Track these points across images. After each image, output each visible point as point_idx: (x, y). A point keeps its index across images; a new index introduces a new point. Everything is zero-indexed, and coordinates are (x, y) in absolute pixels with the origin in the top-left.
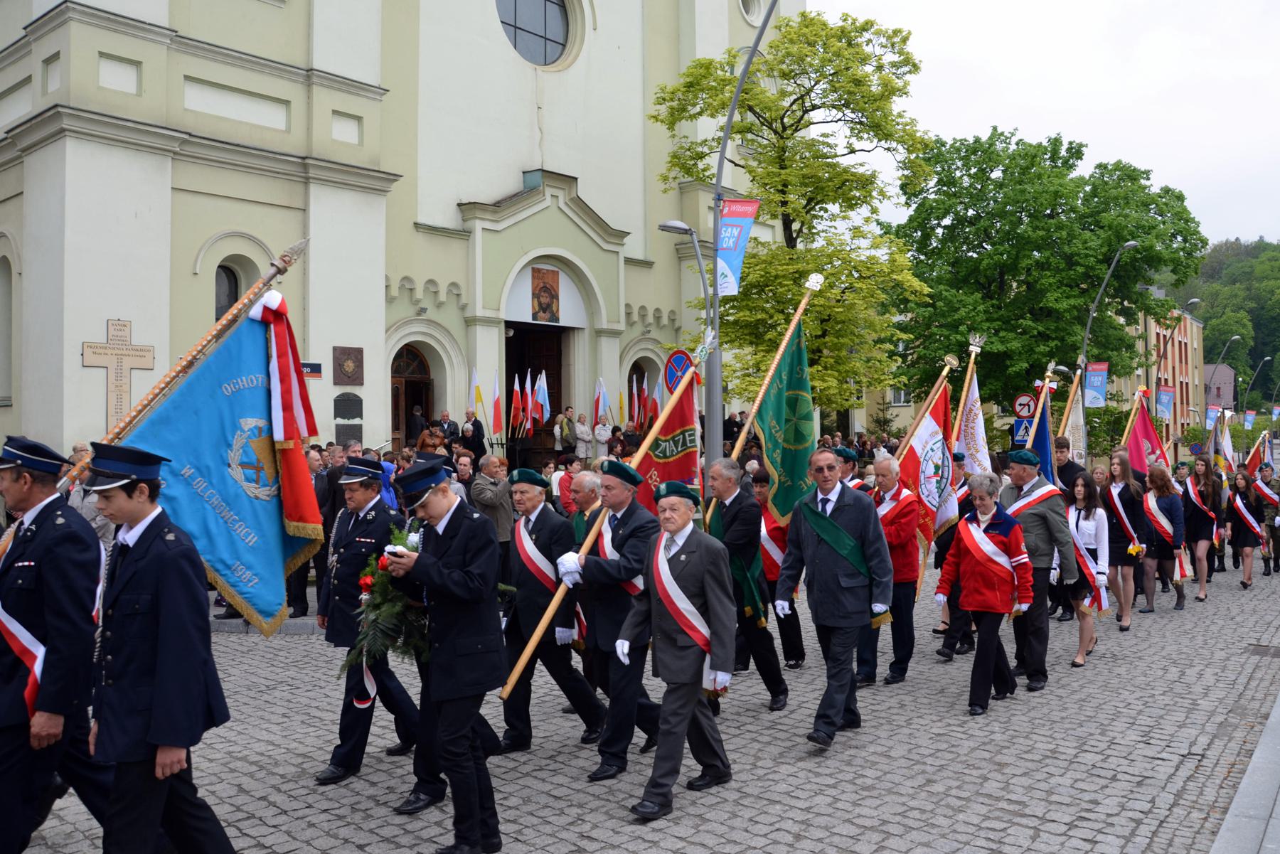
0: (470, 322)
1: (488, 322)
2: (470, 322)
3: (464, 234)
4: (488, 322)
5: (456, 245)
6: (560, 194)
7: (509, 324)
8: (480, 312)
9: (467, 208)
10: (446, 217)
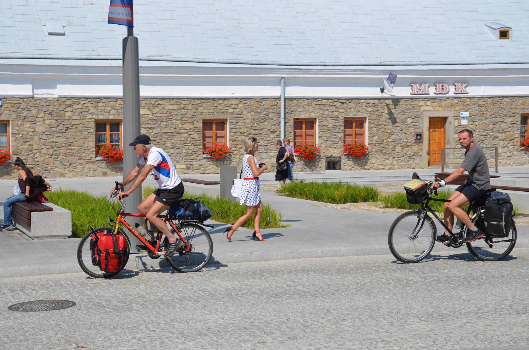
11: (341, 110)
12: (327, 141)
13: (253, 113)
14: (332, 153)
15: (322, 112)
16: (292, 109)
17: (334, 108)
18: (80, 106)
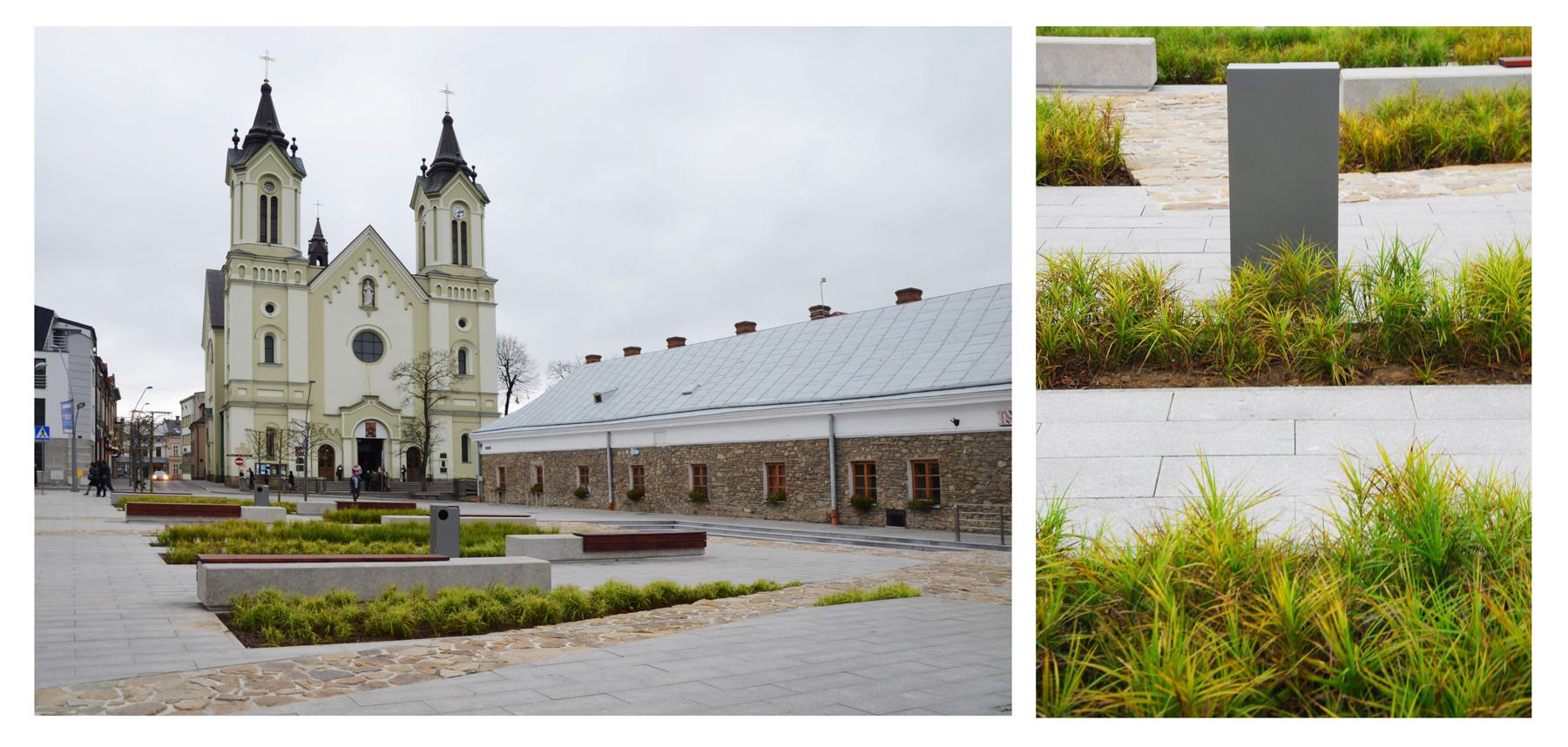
0: (342, 439)
1: (348, 439)
2: (342, 439)
3: (340, 415)
4: (348, 439)
5: (338, 419)
6: (374, 402)
7: (358, 439)
8: (343, 436)
9: (342, 408)
10: (335, 411)
11: (904, 451)
12: (889, 489)
13: (808, 456)
14: (894, 504)
15: (880, 454)
16: (846, 450)
17: (895, 449)
18: (679, 453)
